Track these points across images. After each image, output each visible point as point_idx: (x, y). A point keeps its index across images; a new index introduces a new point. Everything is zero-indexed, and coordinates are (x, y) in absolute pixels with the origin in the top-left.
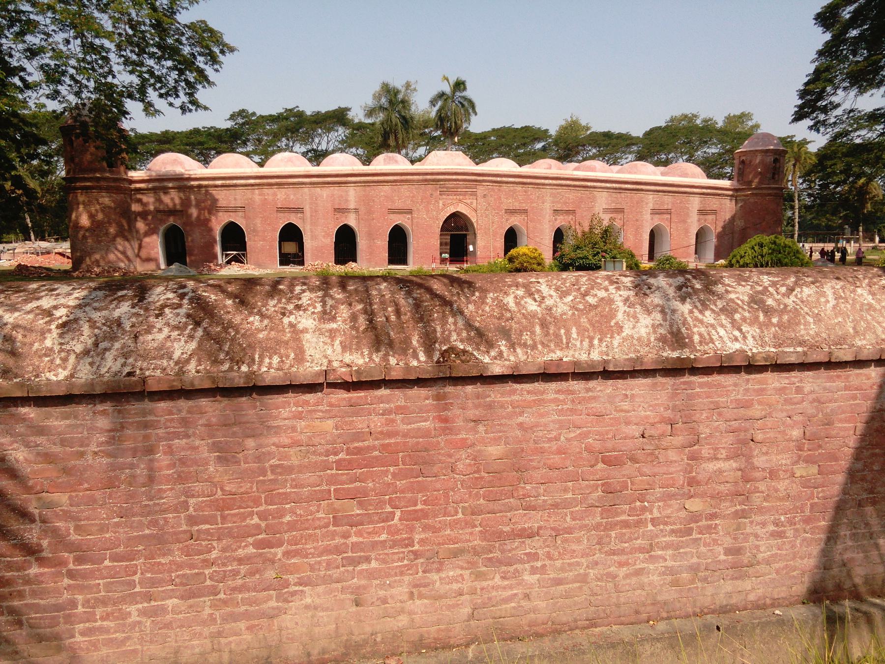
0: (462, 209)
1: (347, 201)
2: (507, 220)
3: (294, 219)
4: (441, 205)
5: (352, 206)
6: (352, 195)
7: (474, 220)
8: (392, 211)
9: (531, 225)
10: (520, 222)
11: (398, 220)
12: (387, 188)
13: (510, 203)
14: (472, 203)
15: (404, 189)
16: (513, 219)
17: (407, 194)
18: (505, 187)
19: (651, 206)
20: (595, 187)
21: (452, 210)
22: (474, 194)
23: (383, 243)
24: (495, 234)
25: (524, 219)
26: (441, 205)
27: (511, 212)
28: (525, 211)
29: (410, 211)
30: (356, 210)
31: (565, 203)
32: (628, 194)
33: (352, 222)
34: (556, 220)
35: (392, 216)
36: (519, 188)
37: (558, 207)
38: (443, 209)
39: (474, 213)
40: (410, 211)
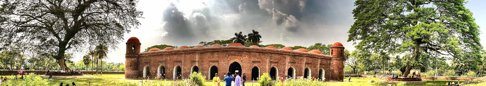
0: (237, 60)
1: (195, 58)
2: (253, 64)
3: (179, 64)
4: (229, 59)
5: (197, 60)
16: (255, 64)
21: (232, 62)
26: (229, 59)
27: (254, 62)
29: (217, 61)
30: (198, 61)
33: (197, 65)
35: (210, 63)
36: (257, 54)
37: (272, 60)
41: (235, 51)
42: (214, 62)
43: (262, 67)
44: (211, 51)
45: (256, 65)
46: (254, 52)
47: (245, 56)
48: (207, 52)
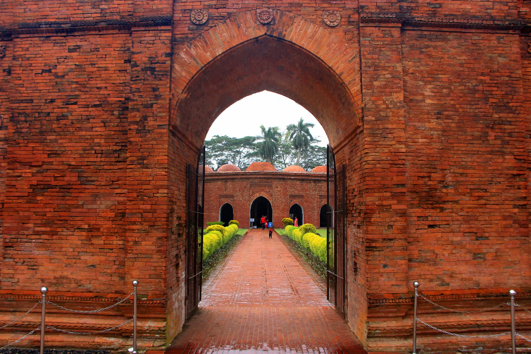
2: (291, 201)
4: (251, 192)
7: (270, 201)
8: (221, 196)
9: (305, 204)
10: (299, 202)
11: (225, 201)
12: (219, 183)
13: (291, 191)
14: (269, 191)
15: (229, 184)
16: (294, 200)
17: (231, 186)
18: (289, 182)
21: (257, 195)
22: (270, 186)
24: (284, 209)
25: (301, 201)
26: (251, 192)
27: (293, 197)
28: (302, 196)
34: (322, 201)
35: (222, 199)
36: (298, 182)
38: (252, 195)
39: (271, 198)
40: (232, 196)
41: (260, 178)
42: (227, 196)
43: (305, 204)
44: (224, 177)
45: (296, 201)
46: (292, 179)
47: (277, 187)
48: (217, 179)
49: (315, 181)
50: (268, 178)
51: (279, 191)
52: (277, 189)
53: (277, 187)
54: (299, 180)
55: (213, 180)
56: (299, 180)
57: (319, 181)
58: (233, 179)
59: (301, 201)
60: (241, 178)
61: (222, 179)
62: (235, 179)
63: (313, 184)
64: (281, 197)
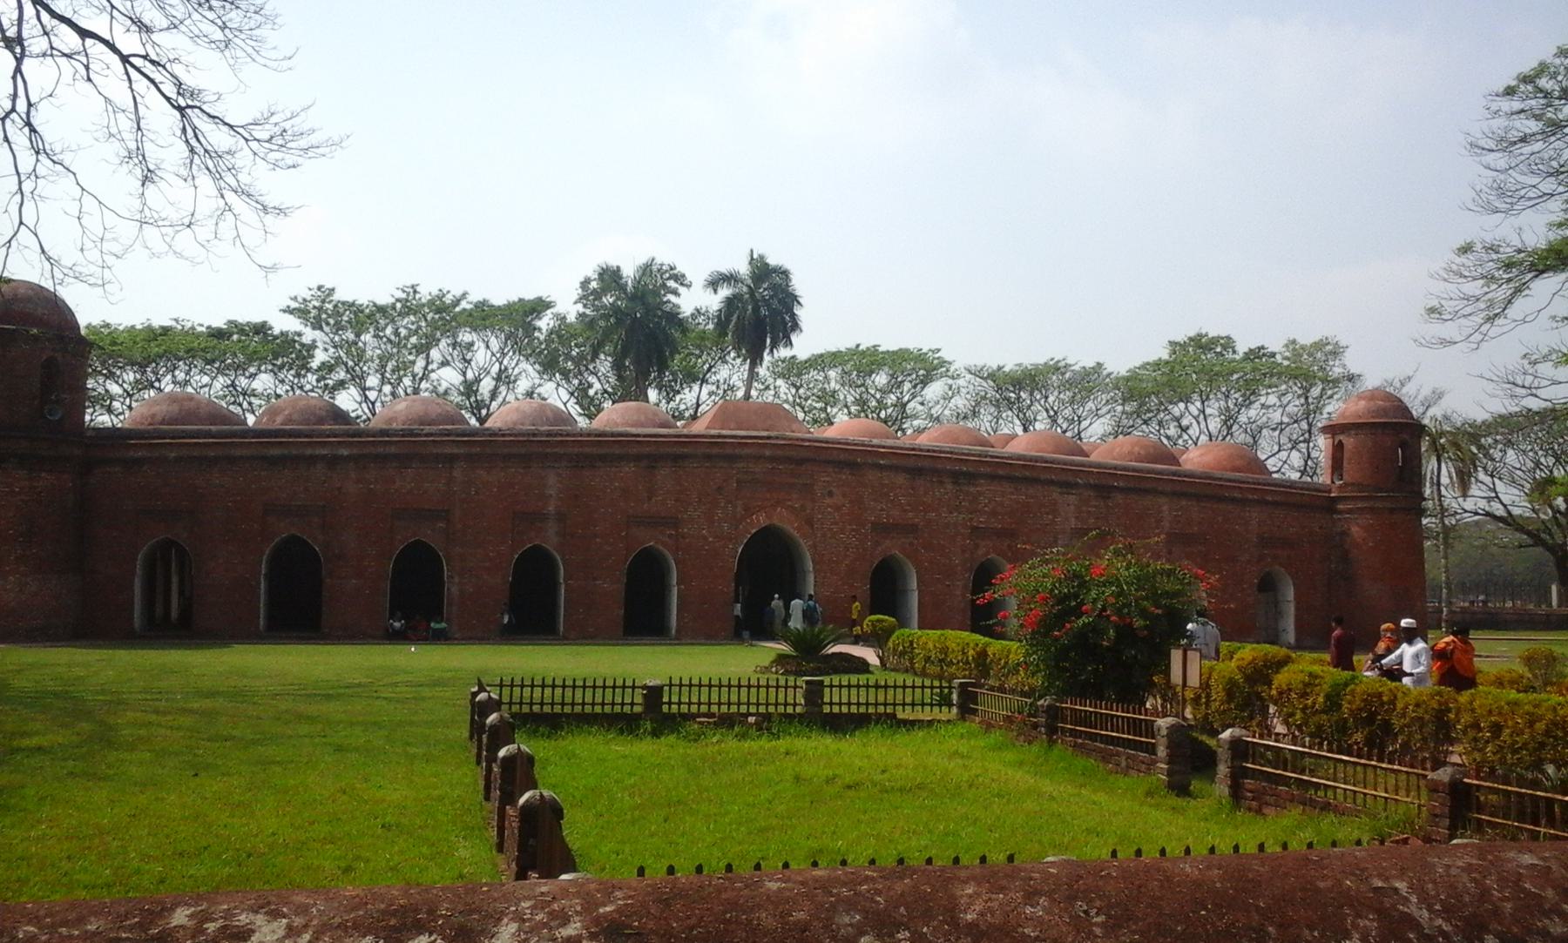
3: (430, 534)
6: (553, 482)
12: (628, 469)
19: (1166, 524)
20: (1052, 482)
21: (761, 520)
23: (611, 587)
27: (884, 529)
28: (913, 529)
31: (994, 513)
32: (1119, 498)
33: (550, 539)
34: (977, 546)
36: (901, 479)
41: (772, 459)
45: (893, 547)
46: (881, 467)
47: (830, 494)
48: (621, 458)
49: (956, 476)
50: (801, 462)
51: (838, 508)
52: (828, 501)
53: (830, 494)
54: (906, 470)
55: (603, 458)
56: (906, 470)
57: (972, 477)
58: (677, 459)
59: (911, 544)
60: (709, 457)
61: (638, 458)
62: (684, 457)
63: (950, 487)
64: (842, 531)
